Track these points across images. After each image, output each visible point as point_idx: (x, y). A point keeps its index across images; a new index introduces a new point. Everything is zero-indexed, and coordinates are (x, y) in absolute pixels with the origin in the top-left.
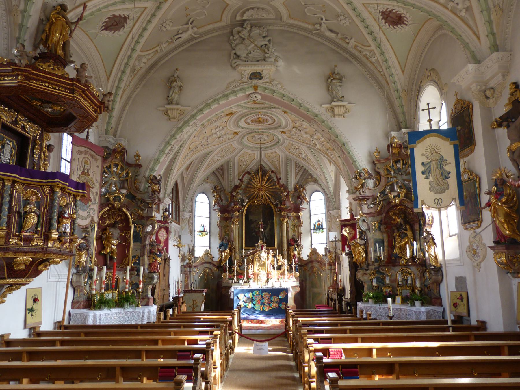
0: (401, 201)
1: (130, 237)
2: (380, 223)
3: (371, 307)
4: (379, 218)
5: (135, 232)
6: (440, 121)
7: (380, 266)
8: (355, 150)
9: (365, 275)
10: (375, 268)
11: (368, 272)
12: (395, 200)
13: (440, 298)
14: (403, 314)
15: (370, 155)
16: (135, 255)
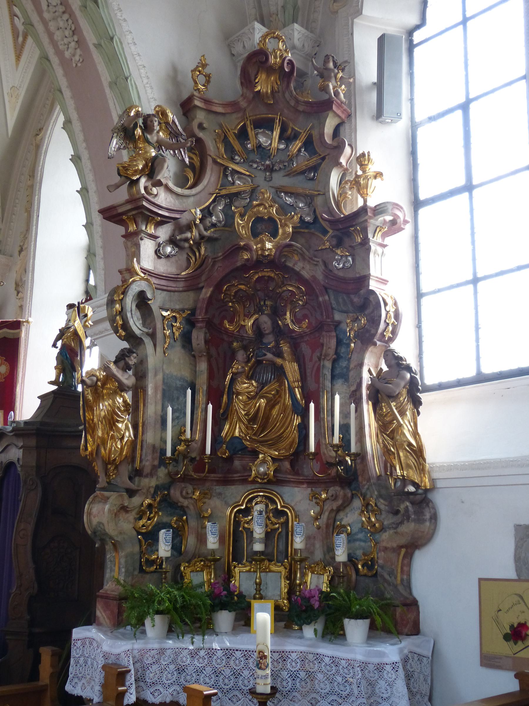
0: (282, 249)
2: (191, 322)
3: (162, 651)
4: (188, 300)
6: (418, 27)
7: (173, 479)
8: (129, 38)
9: (123, 516)
10: (157, 488)
11: (136, 500)
12: (263, 243)
13: (413, 605)
14: (294, 677)
15: (174, 77)
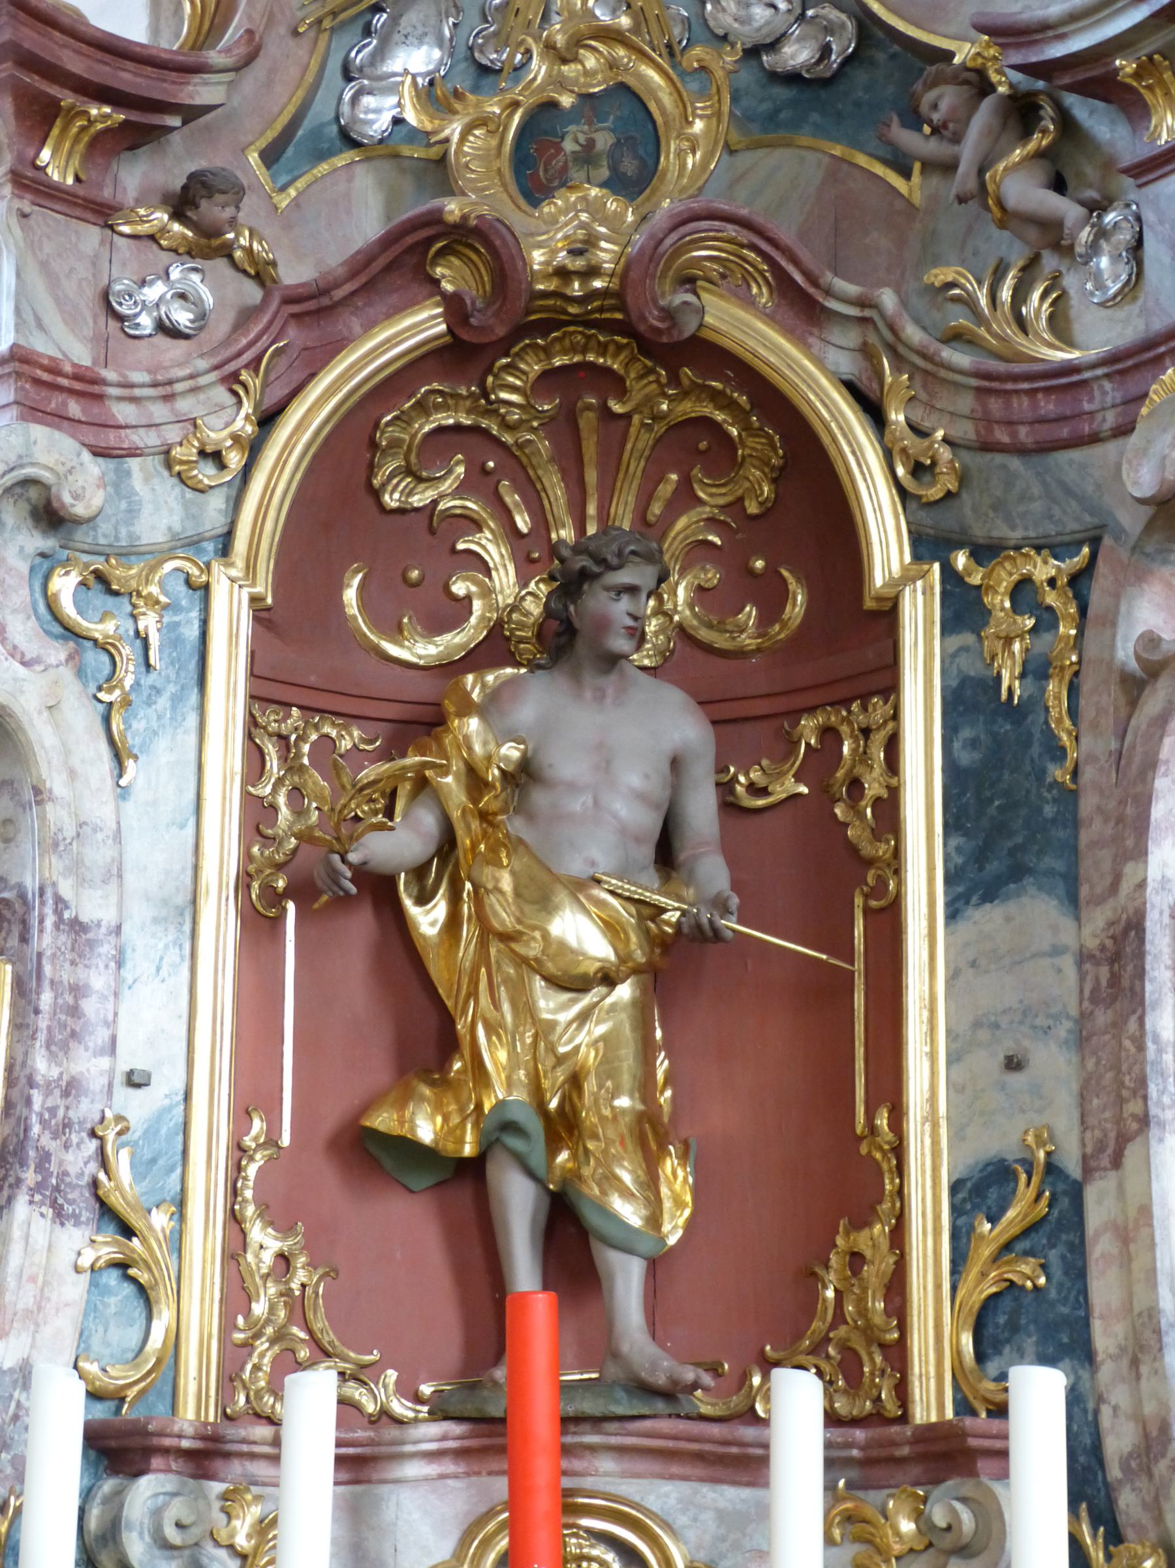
1: (889, 812)
5: (967, 700)
16: (1001, 1140)
